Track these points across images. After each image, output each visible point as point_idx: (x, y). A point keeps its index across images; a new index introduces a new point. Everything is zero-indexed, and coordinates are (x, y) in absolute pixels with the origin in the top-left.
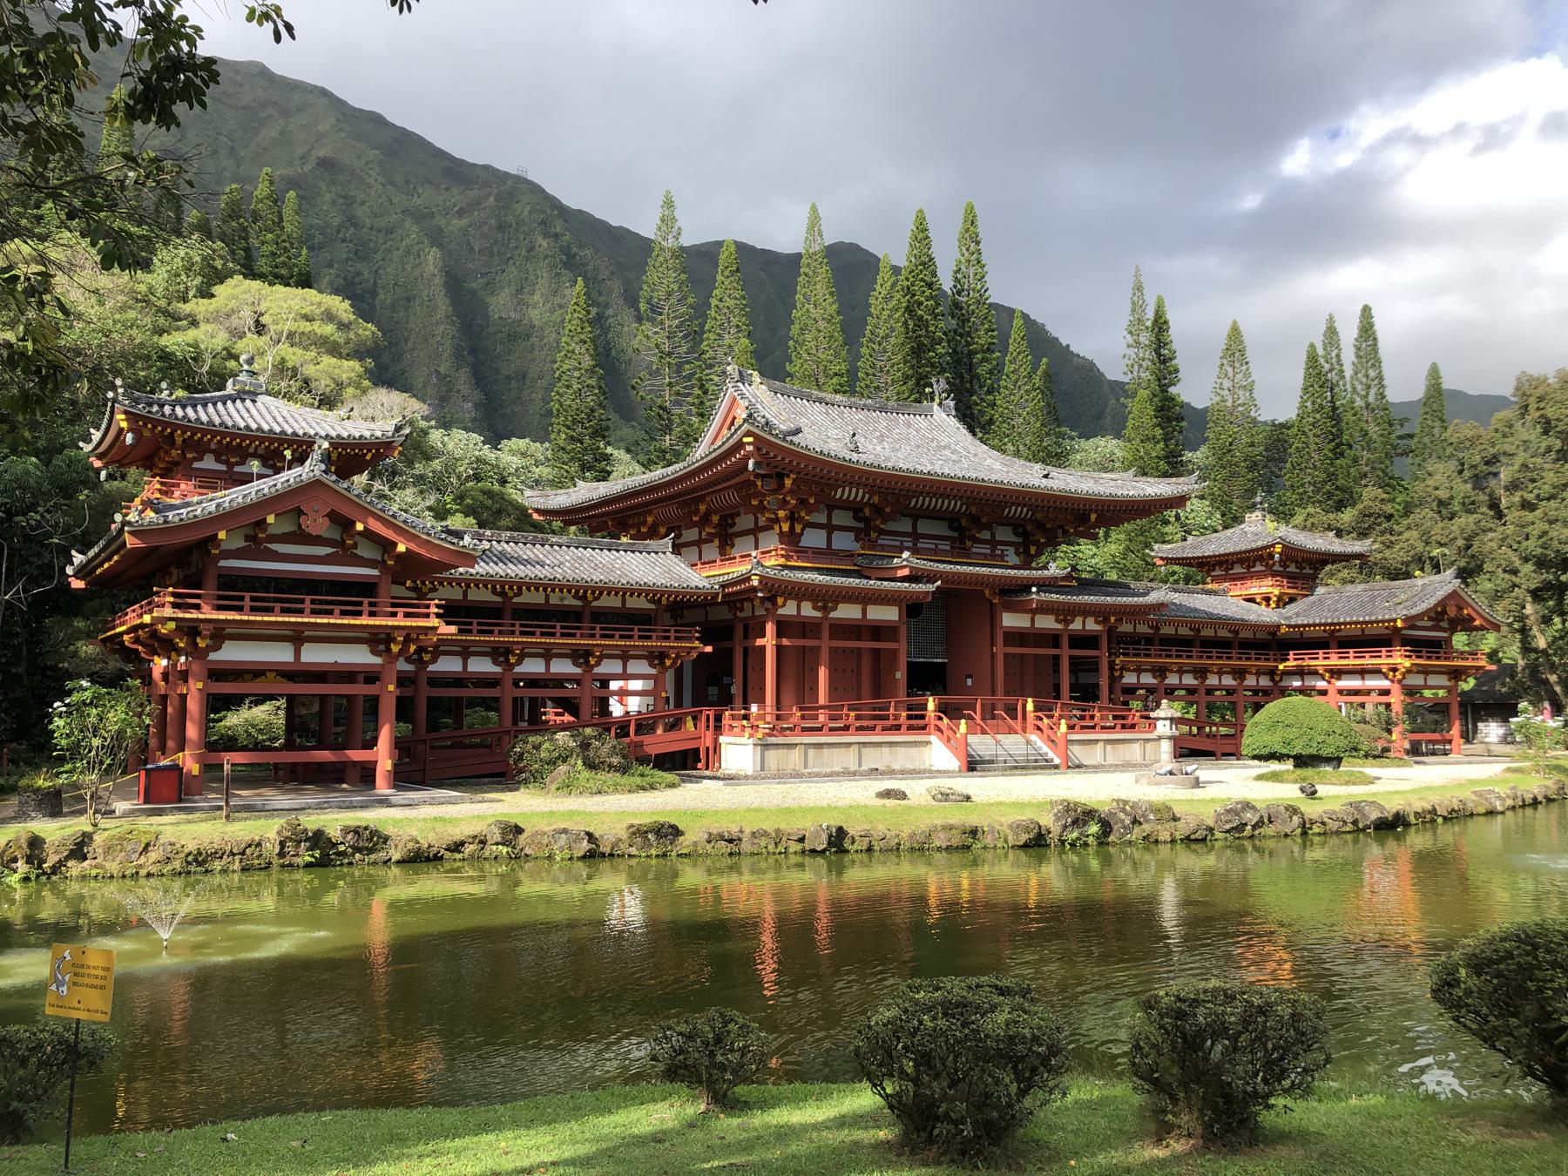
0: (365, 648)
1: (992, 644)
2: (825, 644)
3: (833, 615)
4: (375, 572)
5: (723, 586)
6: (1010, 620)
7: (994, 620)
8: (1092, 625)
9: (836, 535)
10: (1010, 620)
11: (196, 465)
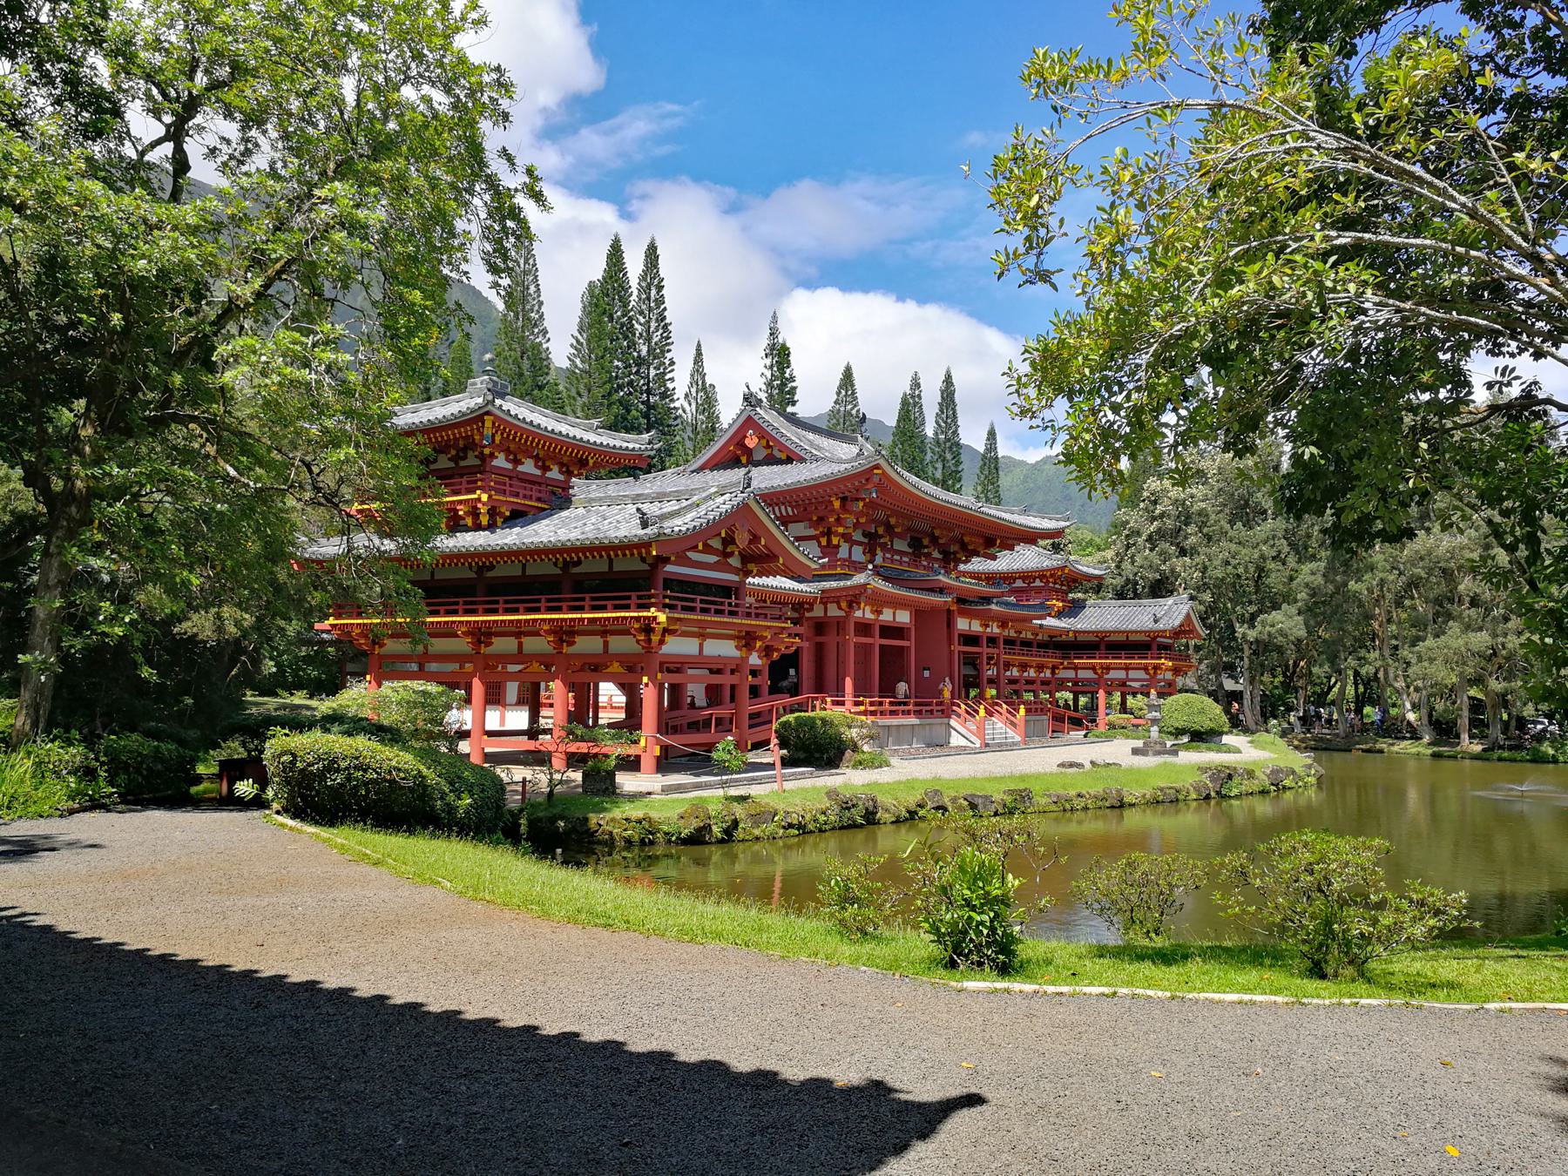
0: (732, 643)
1: (950, 643)
2: (877, 641)
3: (881, 617)
4: (736, 578)
5: (823, 591)
6: (962, 624)
7: (950, 624)
8: (996, 630)
9: (855, 548)
10: (962, 624)
11: (495, 463)
